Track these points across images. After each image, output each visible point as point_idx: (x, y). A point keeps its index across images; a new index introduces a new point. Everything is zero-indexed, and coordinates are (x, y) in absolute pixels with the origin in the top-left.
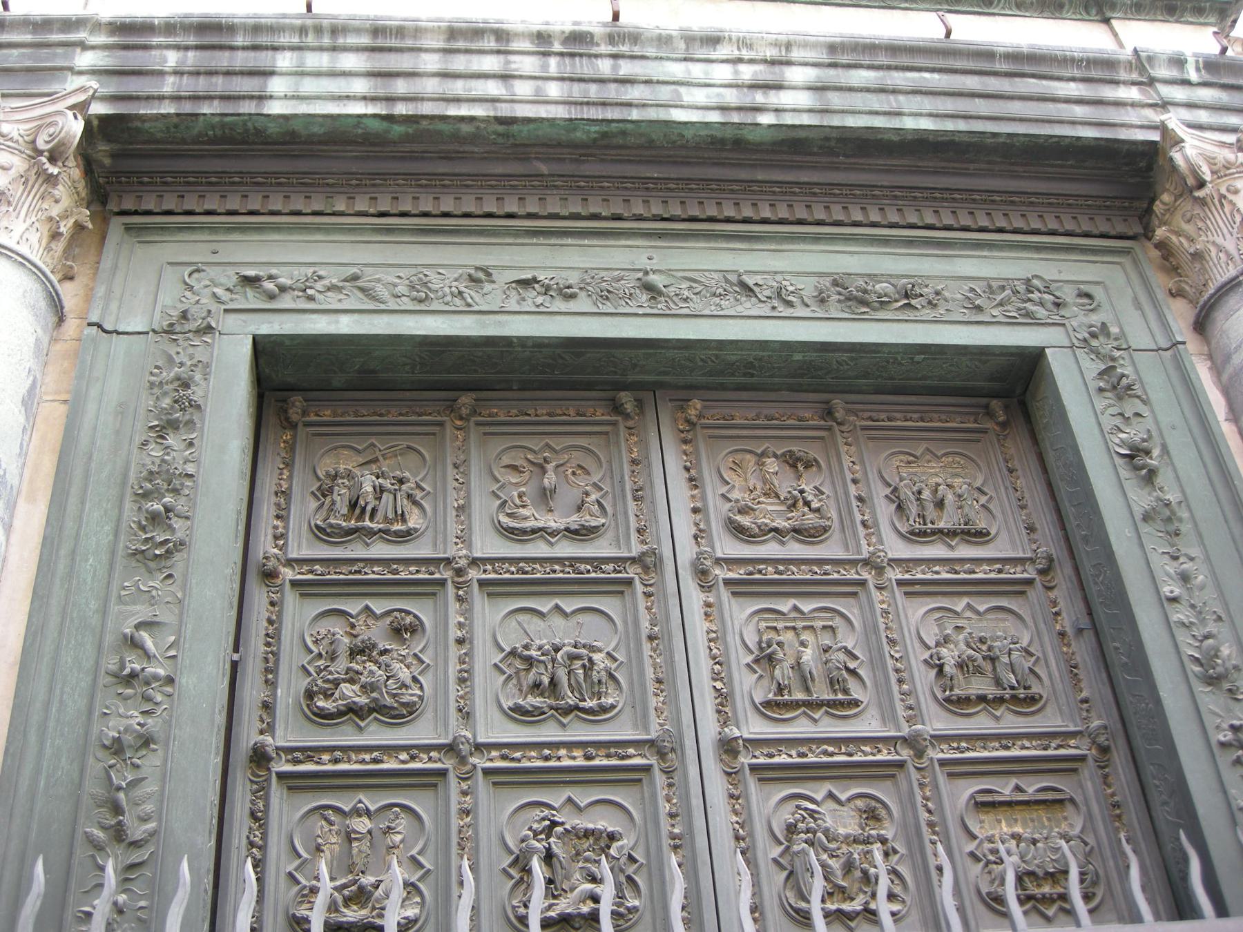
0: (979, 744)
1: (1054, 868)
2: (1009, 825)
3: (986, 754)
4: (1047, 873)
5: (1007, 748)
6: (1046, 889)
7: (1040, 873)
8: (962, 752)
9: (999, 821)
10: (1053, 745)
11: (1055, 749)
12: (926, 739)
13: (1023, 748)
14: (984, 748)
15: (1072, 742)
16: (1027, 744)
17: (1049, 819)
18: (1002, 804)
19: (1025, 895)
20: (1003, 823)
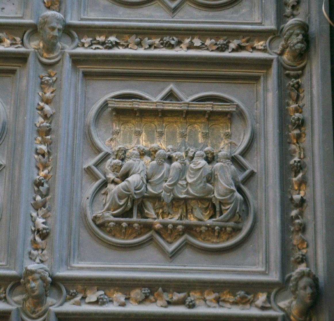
0: (133, 39)
1: (187, 193)
2: (150, 139)
3: (141, 51)
4: (176, 199)
5: (171, 46)
6: (175, 219)
7: (167, 197)
8: (110, 48)
9: (139, 134)
10: (232, 45)
11: (233, 50)
12: (53, 29)
13: (191, 47)
14: (139, 44)
15: (260, 44)
16: (197, 42)
17: (206, 136)
18: (143, 113)
19: (140, 223)
20: (143, 136)
